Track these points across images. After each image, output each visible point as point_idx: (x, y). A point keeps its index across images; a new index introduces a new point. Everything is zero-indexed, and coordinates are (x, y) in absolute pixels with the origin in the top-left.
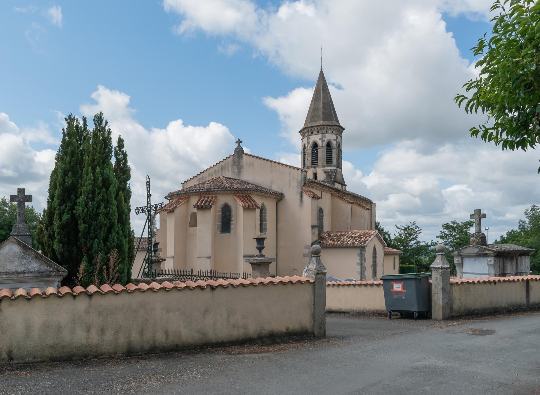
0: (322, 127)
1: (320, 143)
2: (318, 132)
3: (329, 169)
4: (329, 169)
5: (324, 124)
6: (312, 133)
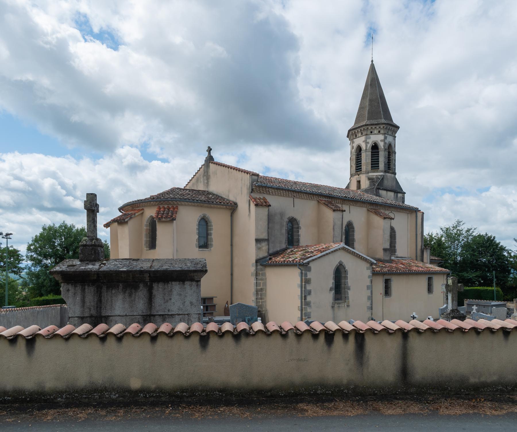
0: (365, 128)
1: (381, 145)
2: (379, 132)
3: (374, 174)
4: (374, 174)
5: (367, 123)
6: (371, 132)
